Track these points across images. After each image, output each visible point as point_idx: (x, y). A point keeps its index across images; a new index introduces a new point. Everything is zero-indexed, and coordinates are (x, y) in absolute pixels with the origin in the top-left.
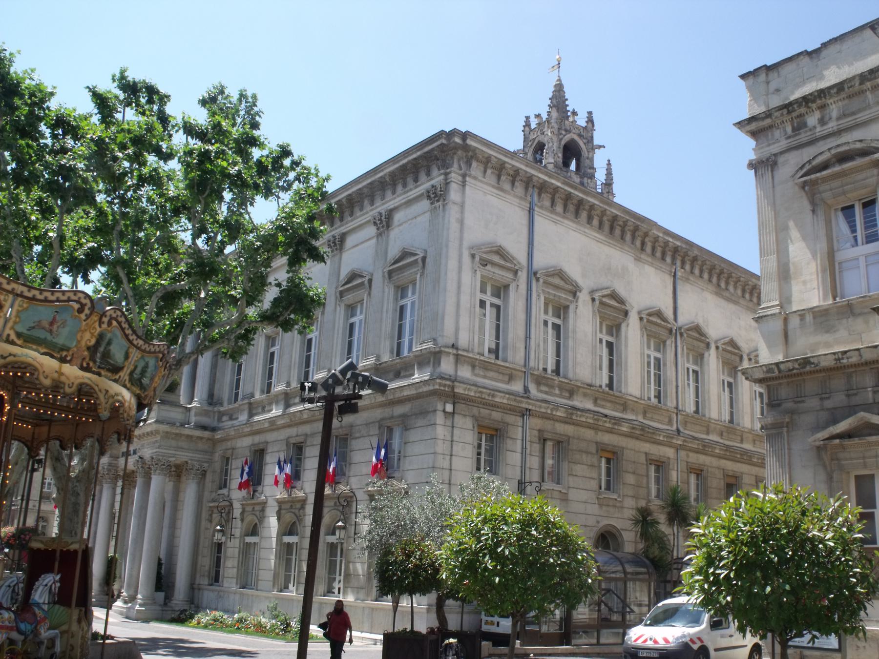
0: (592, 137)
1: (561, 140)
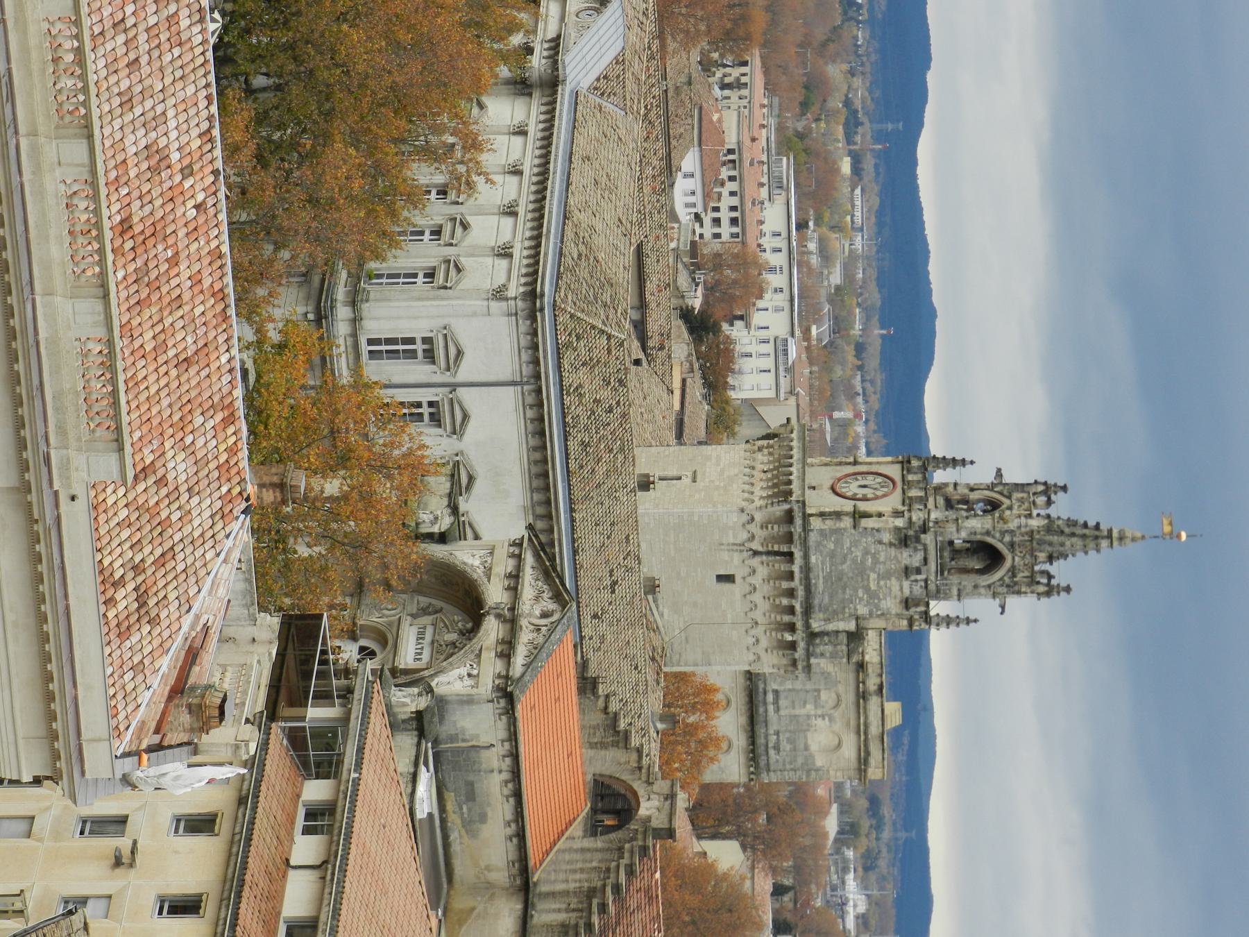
0: (1019, 593)
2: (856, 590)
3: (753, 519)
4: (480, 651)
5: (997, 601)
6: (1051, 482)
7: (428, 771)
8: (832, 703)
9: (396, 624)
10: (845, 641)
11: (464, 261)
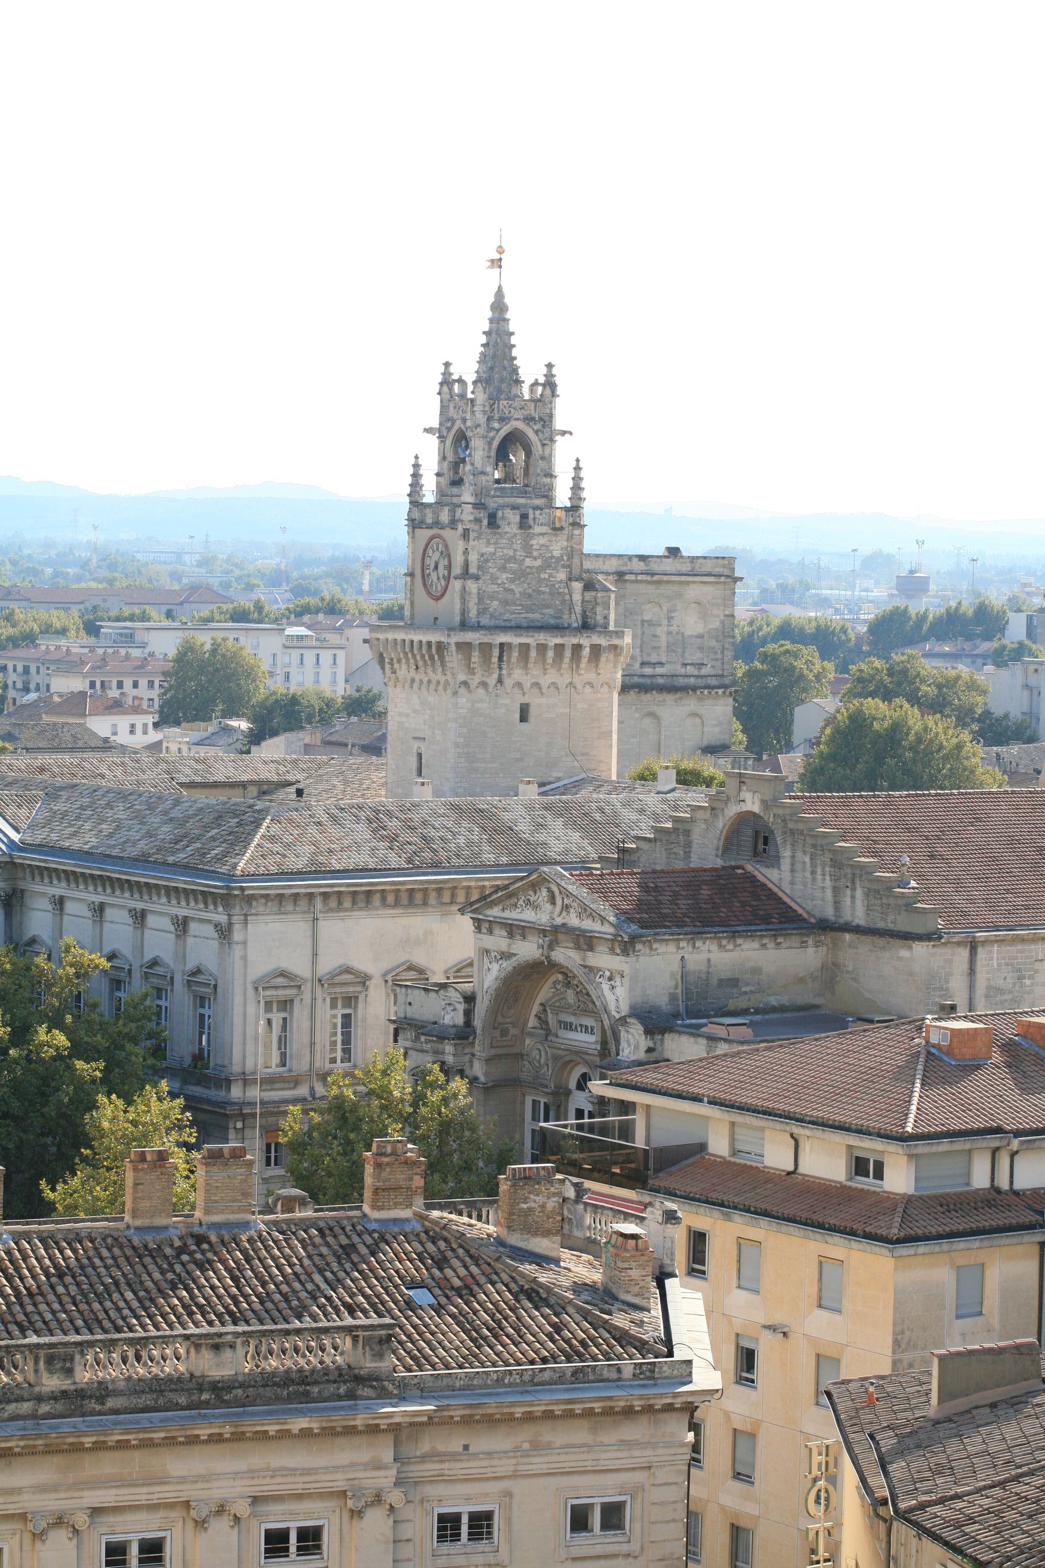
0: (551, 416)
1: (490, 444)
2: (540, 581)
3: (465, 683)
4: (585, 967)
5: (558, 438)
6: (440, 378)
7: (705, 1025)
8: (656, 609)
9: (555, 1051)
10: (593, 593)
11: (190, 966)
